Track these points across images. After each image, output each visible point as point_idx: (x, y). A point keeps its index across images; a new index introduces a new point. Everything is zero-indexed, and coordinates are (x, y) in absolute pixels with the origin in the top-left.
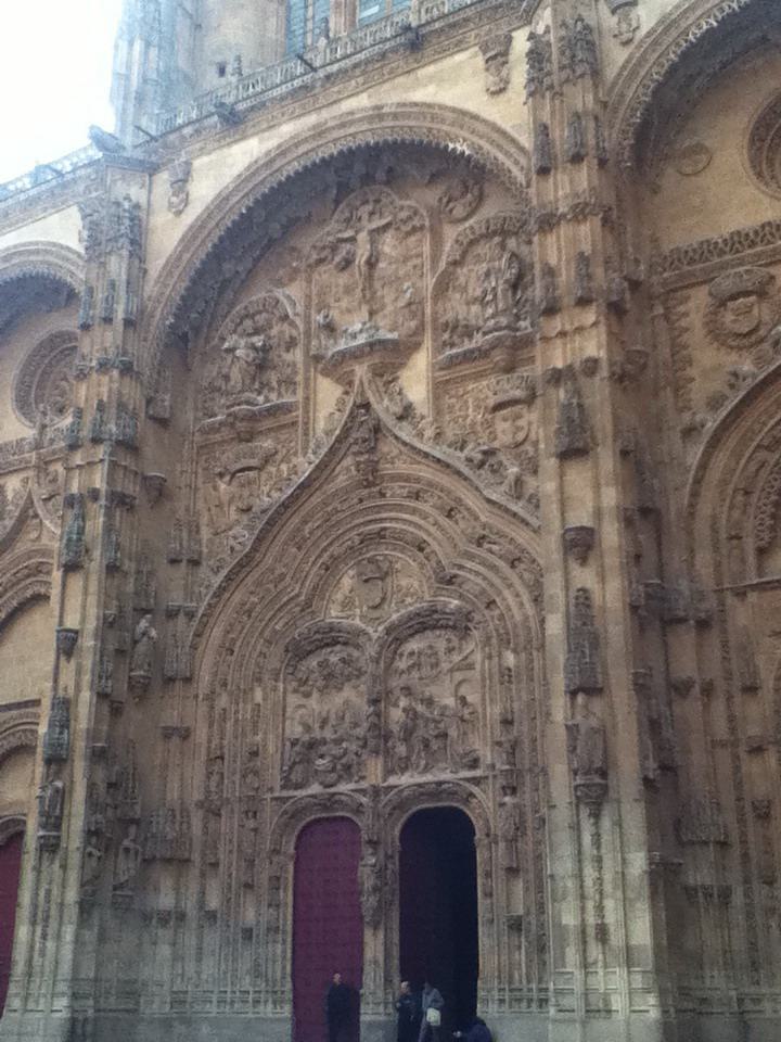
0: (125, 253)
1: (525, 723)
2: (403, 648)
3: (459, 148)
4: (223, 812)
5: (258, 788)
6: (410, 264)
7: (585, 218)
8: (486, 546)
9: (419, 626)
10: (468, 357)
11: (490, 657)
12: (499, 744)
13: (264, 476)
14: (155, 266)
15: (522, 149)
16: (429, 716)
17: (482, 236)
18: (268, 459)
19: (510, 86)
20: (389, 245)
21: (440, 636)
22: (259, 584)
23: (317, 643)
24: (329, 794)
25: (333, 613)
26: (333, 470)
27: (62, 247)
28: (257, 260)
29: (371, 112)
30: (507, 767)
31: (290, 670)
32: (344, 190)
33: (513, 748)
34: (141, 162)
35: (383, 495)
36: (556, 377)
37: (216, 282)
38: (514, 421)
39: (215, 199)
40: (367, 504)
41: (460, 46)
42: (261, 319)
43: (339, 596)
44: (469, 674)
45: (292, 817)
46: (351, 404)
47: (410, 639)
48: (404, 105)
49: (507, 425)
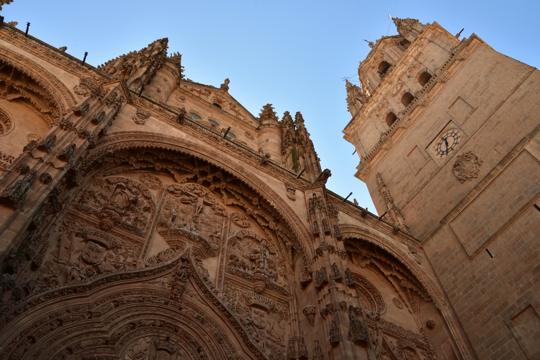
0: (115, 111)
3: (272, 203)
6: (218, 224)
7: (344, 259)
10: (244, 276)
13: (105, 254)
14: (114, 129)
15: (301, 221)
17: (252, 238)
18: (115, 247)
19: (296, 202)
20: (207, 209)
22: (77, 309)
26: (155, 279)
27: (59, 81)
28: (141, 169)
29: (239, 166)
32: (195, 180)
34: (130, 96)
35: (180, 309)
36: (343, 306)
37: (123, 159)
38: (261, 316)
39: (159, 134)
40: (169, 307)
41: (276, 177)
42: (134, 190)
43: (136, 349)
46: (180, 255)
48: (253, 175)
49: (257, 316)
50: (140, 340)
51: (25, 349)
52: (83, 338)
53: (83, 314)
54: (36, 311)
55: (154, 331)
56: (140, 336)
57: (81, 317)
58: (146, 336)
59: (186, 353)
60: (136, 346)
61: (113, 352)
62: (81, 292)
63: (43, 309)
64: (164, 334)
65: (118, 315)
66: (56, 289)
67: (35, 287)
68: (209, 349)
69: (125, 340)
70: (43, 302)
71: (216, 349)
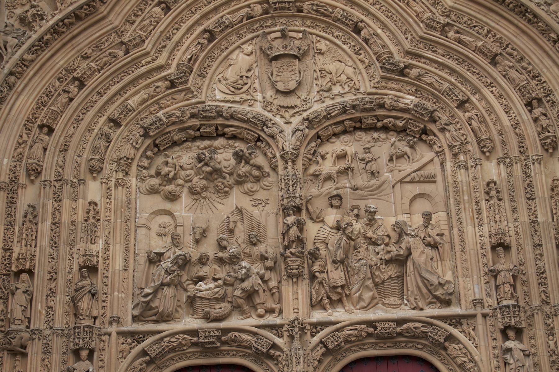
1: (529, 248)
2: (322, 150)
4: (29, 350)
5: (95, 318)
8: (451, 34)
9: (353, 124)
11: (466, 169)
12: (494, 274)
16: (370, 234)
21: (376, 140)
23: (191, 132)
24: (218, 329)
25: (219, 96)
30: (512, 302)
31: (146, 163)
33: (514, 277)
43: (231, 74)
44: (427, 188)
45: (148, 363)
47: (334, 139)
50: (234, 56)
51: (43, 148)
52: (129, 93)
53: (110, 51)
54: (30, 80)
55: (255, 27)
56: (231, 48)
57: (110, 57)
58: (243, 44)
59: (331, 45)
60: (230, 68)
61: (191, 95)
62: (90, 14)
63: (41, 73)
64: (276, 25)
65: (177, 26)
66: (42, 29)
67: (7, 42)
68: (378, 19)
69: (206, 65)
70: (32, 61)
71: (394, 12)
